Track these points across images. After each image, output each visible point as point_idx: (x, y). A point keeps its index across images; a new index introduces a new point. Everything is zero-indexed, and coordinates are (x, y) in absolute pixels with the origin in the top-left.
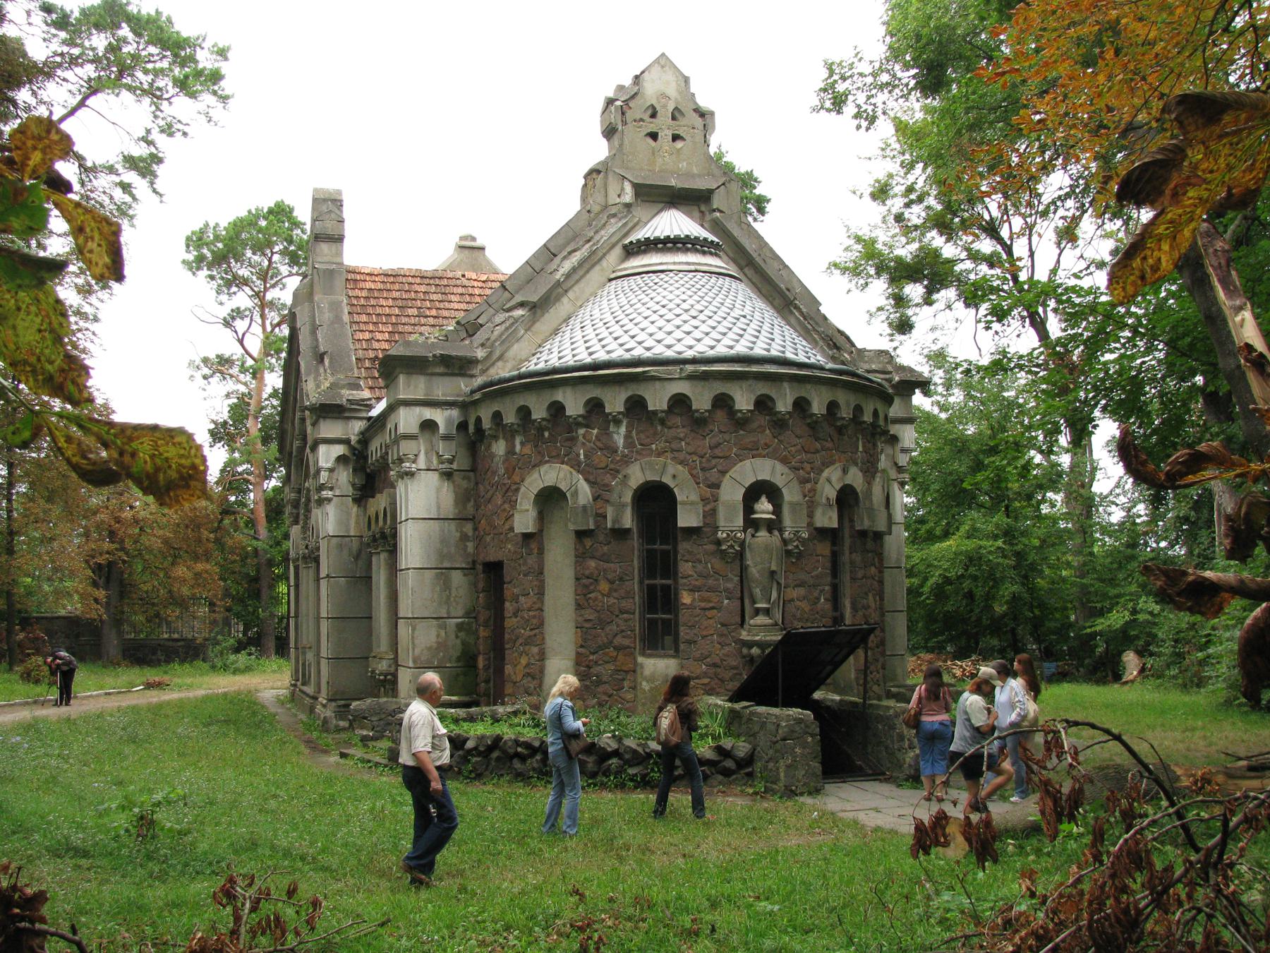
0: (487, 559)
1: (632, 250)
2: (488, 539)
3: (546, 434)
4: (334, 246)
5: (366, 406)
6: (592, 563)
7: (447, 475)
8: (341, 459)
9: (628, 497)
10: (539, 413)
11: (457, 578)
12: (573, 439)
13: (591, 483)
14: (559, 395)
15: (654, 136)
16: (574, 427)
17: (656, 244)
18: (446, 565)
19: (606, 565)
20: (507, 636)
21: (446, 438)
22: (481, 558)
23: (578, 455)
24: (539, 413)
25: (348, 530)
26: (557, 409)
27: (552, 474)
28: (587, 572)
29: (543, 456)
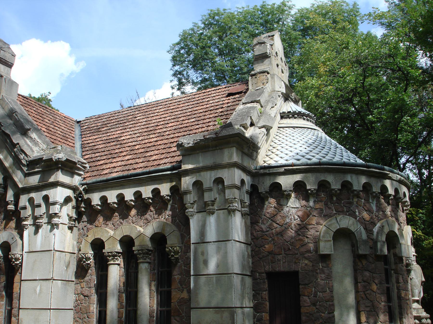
0: (277, 269)
1: (283, 116)
2: (279, 257)
3: (335, 199)
4: (7, 68)
5: (85, 167)
6: (367, 274)
7: (243, 215)
8: (67, 200)
9: (384, 239)
10: (336, 185)
11: (248, 281)
12: (351, 203)
13: (365, 229)
14: (349, 178)
15: (278, 65)
16: (351, 197)
17: (303, 116)
18: (244, 273)
19: (374, 275)
20: (303, 318)
21: (247, 192)
22: (268, 268)
23: (355, 212)
24: (336, 185)
25: (64, 248)
26: (346, 185)
27: (346, 222)
28: (365, 279)
29: (332, 210)
